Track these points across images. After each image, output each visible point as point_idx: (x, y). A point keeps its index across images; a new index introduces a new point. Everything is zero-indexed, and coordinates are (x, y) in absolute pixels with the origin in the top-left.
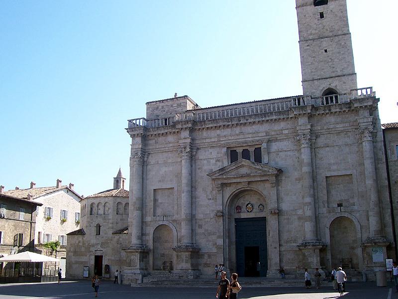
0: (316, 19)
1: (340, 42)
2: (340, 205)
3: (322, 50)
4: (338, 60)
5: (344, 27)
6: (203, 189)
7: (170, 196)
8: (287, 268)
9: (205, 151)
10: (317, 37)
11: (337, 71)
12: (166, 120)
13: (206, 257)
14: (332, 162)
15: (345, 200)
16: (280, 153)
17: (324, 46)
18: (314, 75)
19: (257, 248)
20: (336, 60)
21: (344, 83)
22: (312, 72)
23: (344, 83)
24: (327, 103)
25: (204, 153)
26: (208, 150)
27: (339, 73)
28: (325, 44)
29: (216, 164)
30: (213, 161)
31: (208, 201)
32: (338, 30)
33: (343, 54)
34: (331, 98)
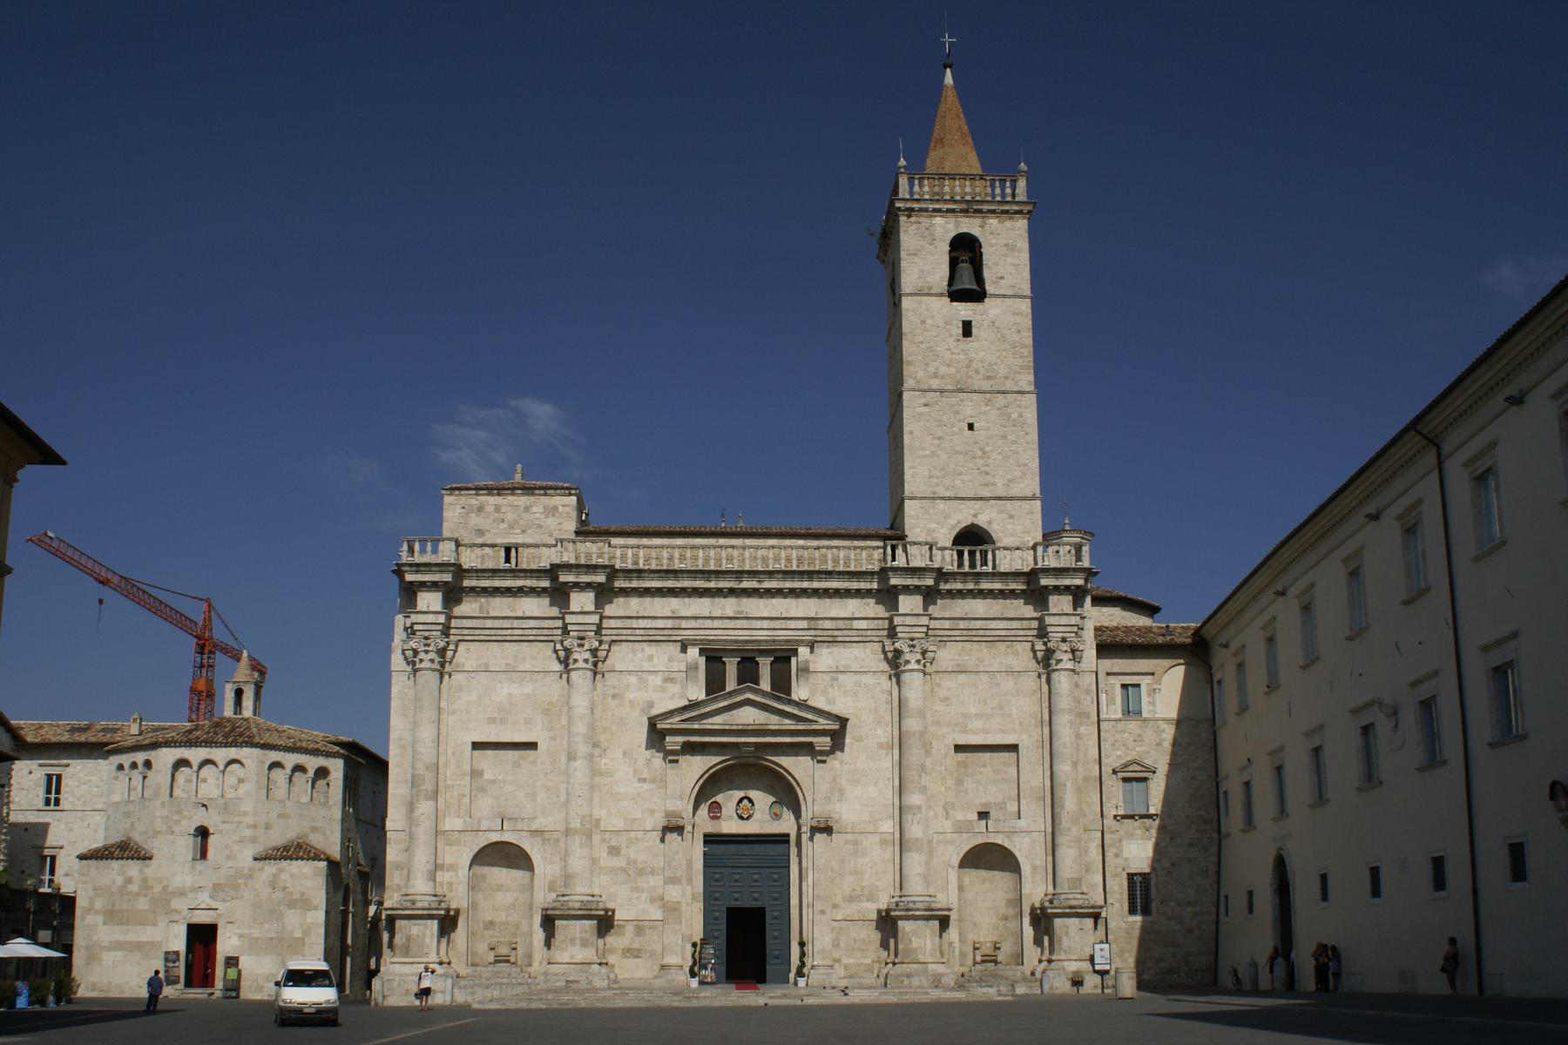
0: (951, 336)
1: (1009, 410)
2: (983, 815)
3: (961, 424)
4: (1000, 457)
5: (1020, 373)
6: (625, 752)
7: (519, 766)
8: (851, 961)
9: (634, 651)
10: (950, 387)
11: (994, 485)
12: (508, 550)
13: (629, 930)
14: (973, 711)
15: (995, 803)
16: (841, 677)
17: (969, 413)
18: (937, 485)
19: (761, 912)
20: (995, 455)
21: (1011, 517)
22: (931, 477)
23: (1011, 517)
24: (972, 565)
25: (631, 656)
26: (643, 650)
27: (1001, 493)
28: (970, 408)
29: (663, 689)
30: (657, 680)
31: (637, 785)
32: (1006, 378)
33: (1014, 442)
34: (984, 554)
